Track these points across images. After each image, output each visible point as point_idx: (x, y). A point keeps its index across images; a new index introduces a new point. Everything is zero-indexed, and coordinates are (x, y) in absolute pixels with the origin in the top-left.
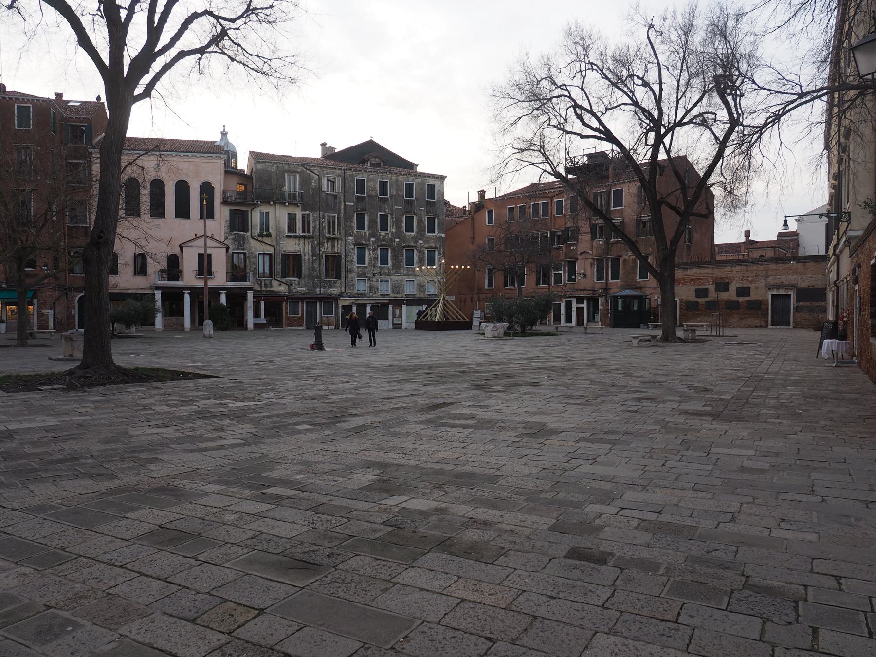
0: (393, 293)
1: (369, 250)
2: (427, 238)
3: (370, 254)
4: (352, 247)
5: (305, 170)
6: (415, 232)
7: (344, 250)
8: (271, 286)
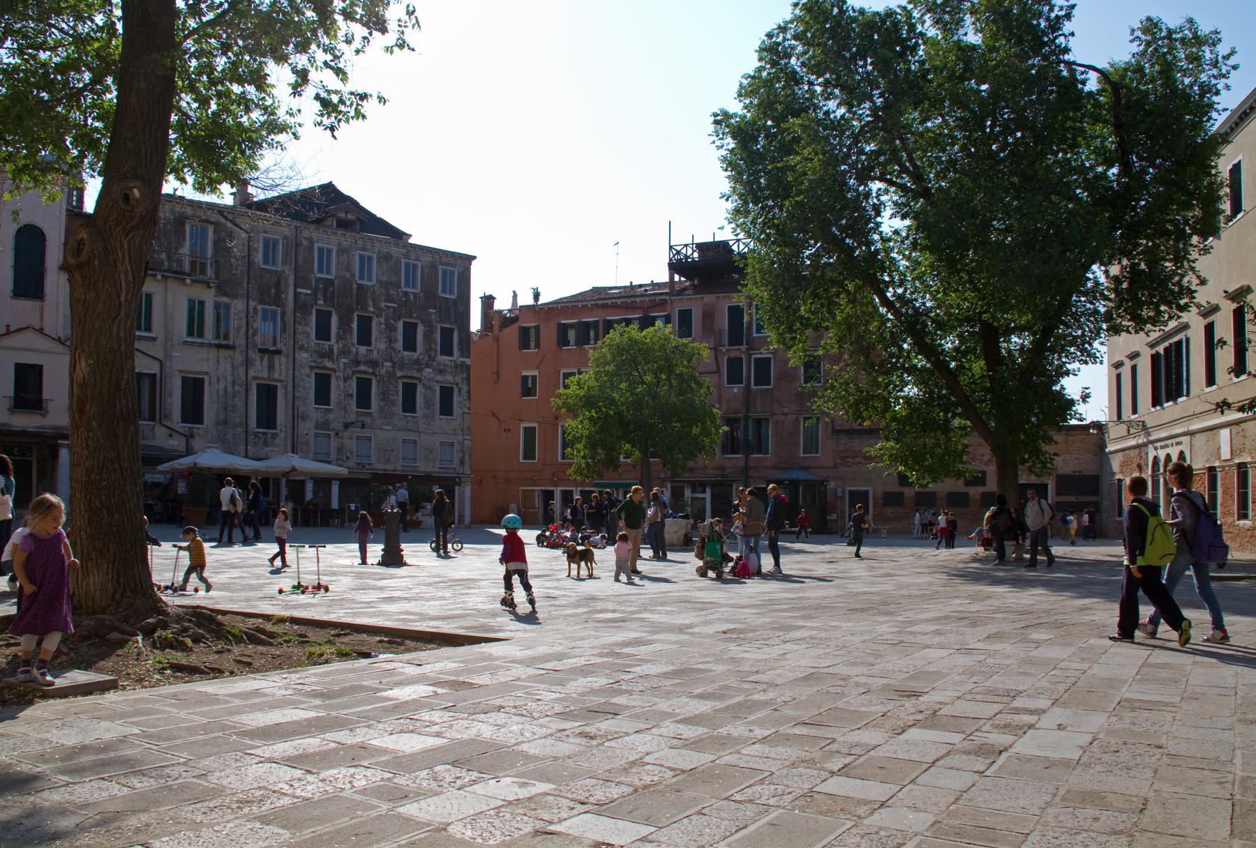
0: (378, 462)
1: (337, 377)
2: (439, 364)
3: (339, 386)
4: (307, 370)
5: (223, 221)
7: (291, 376)
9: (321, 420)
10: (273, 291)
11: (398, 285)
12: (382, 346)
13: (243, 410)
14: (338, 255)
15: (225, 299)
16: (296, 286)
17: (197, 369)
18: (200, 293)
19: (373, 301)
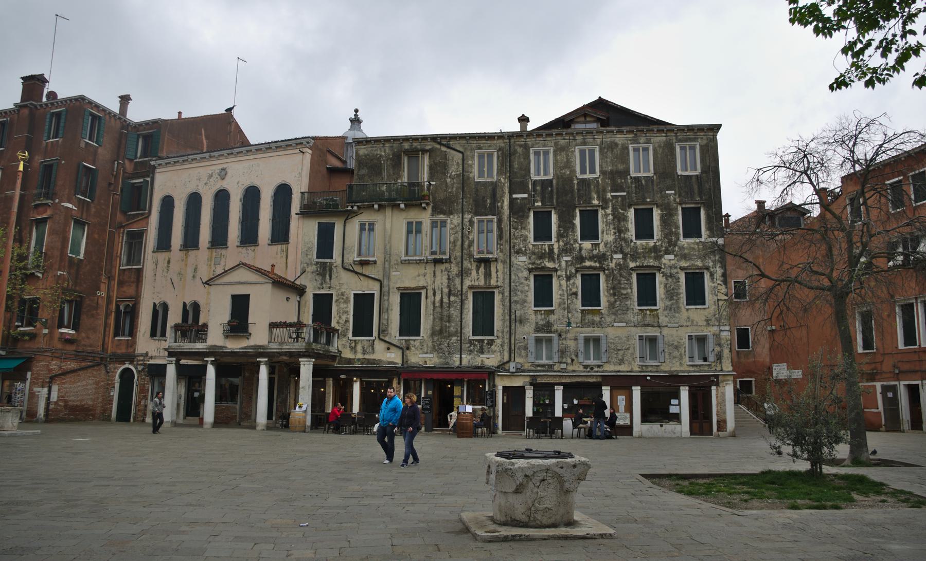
1: (559, 277)
2: (682, 248)
3: (560, 285)
4: (526, 273)
5: (438, 146)
6: (656, 237)
8: (373, 351)
9: (541, 323)
10: (489, 201)
11: (627, 172)
12: (610, 238)
13: (458, 319)
14: (555, 155)
15: (442, 217)
16: (511, 193)
17: (413, 285)
18: (414, 215)
19: (598, 193)
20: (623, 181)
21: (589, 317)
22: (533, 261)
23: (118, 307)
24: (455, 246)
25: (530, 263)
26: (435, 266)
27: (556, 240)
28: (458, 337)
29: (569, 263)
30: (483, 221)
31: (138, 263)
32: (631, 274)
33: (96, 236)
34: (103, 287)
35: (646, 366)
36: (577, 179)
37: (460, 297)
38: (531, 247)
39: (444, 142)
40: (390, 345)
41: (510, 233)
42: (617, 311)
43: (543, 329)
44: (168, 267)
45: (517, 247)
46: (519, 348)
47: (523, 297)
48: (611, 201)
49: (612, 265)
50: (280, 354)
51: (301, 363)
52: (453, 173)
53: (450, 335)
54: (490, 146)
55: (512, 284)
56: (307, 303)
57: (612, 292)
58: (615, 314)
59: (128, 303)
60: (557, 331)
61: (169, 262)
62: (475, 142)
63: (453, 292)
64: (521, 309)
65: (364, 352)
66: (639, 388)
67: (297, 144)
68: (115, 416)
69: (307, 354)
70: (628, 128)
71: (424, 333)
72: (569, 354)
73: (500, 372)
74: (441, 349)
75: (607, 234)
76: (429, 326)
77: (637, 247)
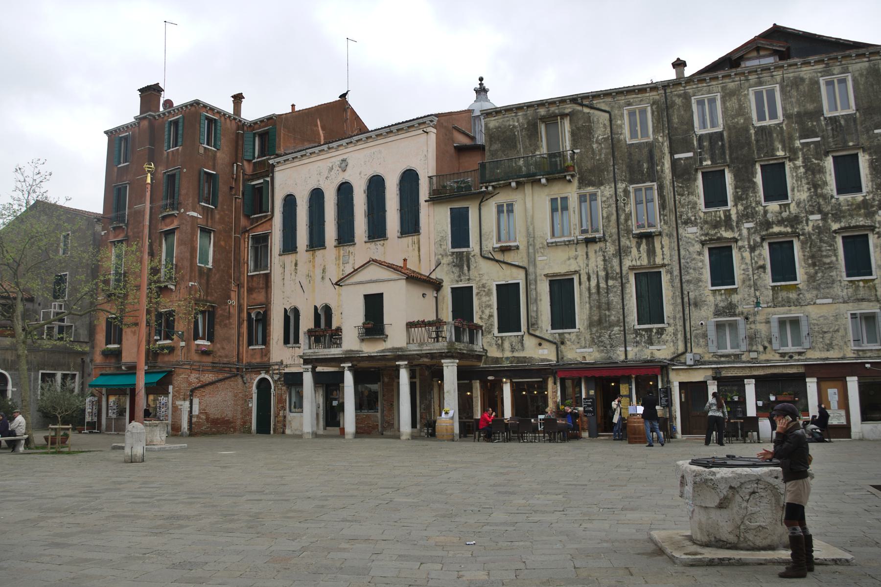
3: (743, 258)
4: (698, 247)
5: (580, 108)
6: (864, 189)
7: (676, 258)
9: (722, 304)
10: (645, 165)
11: (820, 112)
12: (804, 195)
13: (620, 306)
14: (724, 102)
15: (591, 189)
16: (672, 154)
18: (558, 190)
19: (783, 142)
20: (815, 123)
21: (783, 294)
22: (706, 231)
23: (249, 314)
24: (609, 221)
25: (703, 235)
26: (587, 246)
27: (733, 203)
28: (620, 326)
29: (752, 231)
30: (640, 189)
31: (266, 268)
32: (835, 237)
33: (222, 243)
34: (233, 295)
35: (863, 351)
36: (755, 127)
37: (620, 280)
38: (702, 215)
39: (586, 102)
40: (542, 341)
41: (675, 201)
42: (819, 285)
43: (724, 312)
44: (296, 269)
45: (684, 217)
46: (696, 337)
47: (697, 276)
48: (802, 150)
49: (809, 229)
50: (421, 356)
51: (444, 365)
52: (600, 137)
53: (611, 325)
54: (641, 101)
55: (682, 261)
56: (446, 298)
57: (810, 262)
58: (817, 288)
59: (258, 310)
60: (742, 313)
61: (296, 265)
62: (623, 98)
63: (610, 275)
64: (695, 290)
65: (513, 350)
66: (856, 378)
67: (419, 124)
68: (255, 428)
69: (450, 355)
70: (816, 58)
71: (579, 324)
72: (759, 340)
73: (674, 365)
74: (602, 342)
75: (798, 191)
76: (585, 317)
77: (840, 204)
